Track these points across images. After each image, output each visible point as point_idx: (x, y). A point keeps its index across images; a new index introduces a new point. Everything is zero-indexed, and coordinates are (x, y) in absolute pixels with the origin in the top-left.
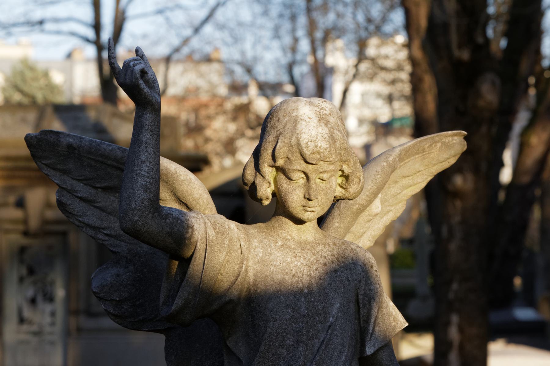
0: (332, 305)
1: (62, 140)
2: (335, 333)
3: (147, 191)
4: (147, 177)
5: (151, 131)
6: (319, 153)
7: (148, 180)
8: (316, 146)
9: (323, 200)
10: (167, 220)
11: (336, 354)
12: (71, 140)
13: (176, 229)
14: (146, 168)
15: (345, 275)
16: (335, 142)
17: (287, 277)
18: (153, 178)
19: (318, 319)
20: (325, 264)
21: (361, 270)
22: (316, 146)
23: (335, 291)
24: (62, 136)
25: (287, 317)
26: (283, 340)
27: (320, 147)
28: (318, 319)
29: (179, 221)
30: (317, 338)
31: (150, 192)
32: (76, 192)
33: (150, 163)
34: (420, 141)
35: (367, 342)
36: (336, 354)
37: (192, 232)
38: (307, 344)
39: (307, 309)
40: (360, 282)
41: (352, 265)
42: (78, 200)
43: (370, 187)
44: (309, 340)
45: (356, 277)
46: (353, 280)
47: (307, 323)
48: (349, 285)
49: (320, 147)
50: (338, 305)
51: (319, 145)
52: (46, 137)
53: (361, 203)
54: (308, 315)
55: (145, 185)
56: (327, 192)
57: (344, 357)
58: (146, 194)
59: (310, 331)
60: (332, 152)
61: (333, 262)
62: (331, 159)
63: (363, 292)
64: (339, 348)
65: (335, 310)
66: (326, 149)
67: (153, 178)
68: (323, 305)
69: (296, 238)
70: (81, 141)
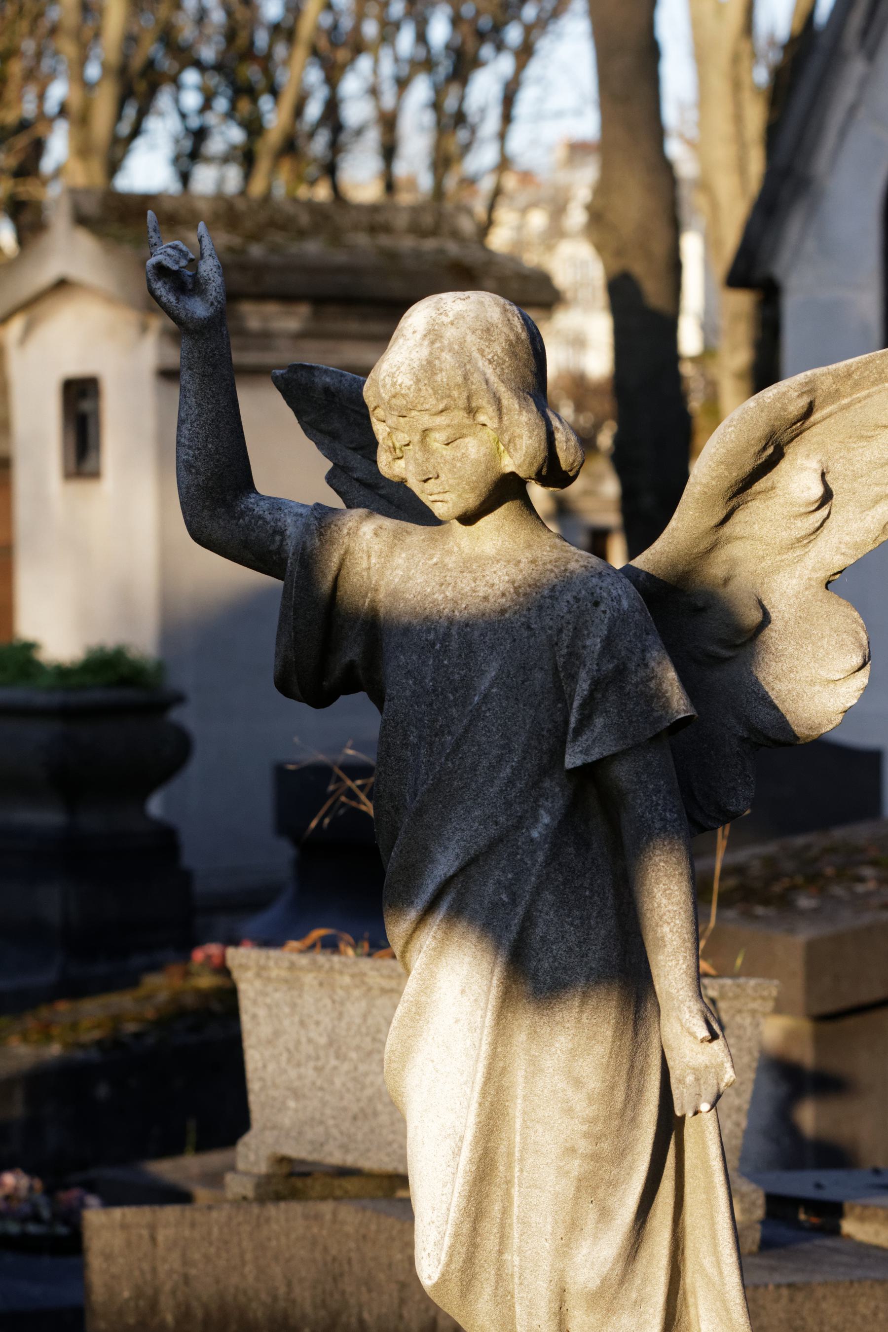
0: (483, 673)
1: (317, 380)
2: (481, 724)
3: (190, 471)
4: (190, 447)
5: (189, 368)
6: (403, 396)
7: (191, 452)
8: (394, 384)
9: (451, 481)
10: (241, 521)
11: (485, 763)
12: (328, 380)
13: (253, 536)
14: (187, 432)
15: (523, 619)
16: (434, 374)
17: (415, 622)
18: (199, 449)
19: (452, 698)
20: (486, 598)
21: (565, 610)
22: (394, 384)
23: (493, 648)
24: (316, 373)
25: (408, 693)
26: (406, 736)
27: (400, 385)
28: (452, 698)
29: (260, 522)
30: (449, 733)
31: (198, 473)
32: (352, 469)
33: (192, 423)
34: (882, 355)
35: (569, 745)
36: (485, 763)
37: (282, 541)
38: (431, 744)
39: (433, 679)
40: (560, 631)
41: (547, 600)
42: (357, 485)
43: (713, 450)
44: (436, 735)
45: (551, 623)
46: (543, 628)
47: (431, 704)
48: (528, 638)
49: (400, 385)
50: (493, 674)
51: (399, 382)
52: (295, 377)
53: (704, 481)
54: (434, 691)
55: (188, 461)
56: (454, 467)
57: (508, 770)
58: (191, 477)
59: (438, 720)
60: (423, 393)
61: (503, 595)
62: (427, 406)
63: (564, 651)
64: (496, 752)
65: (484, 684)
66: (409, 389)
67: (199, 449)
68: (462, 673)
69: (466, 551)
70: (341, 381)
